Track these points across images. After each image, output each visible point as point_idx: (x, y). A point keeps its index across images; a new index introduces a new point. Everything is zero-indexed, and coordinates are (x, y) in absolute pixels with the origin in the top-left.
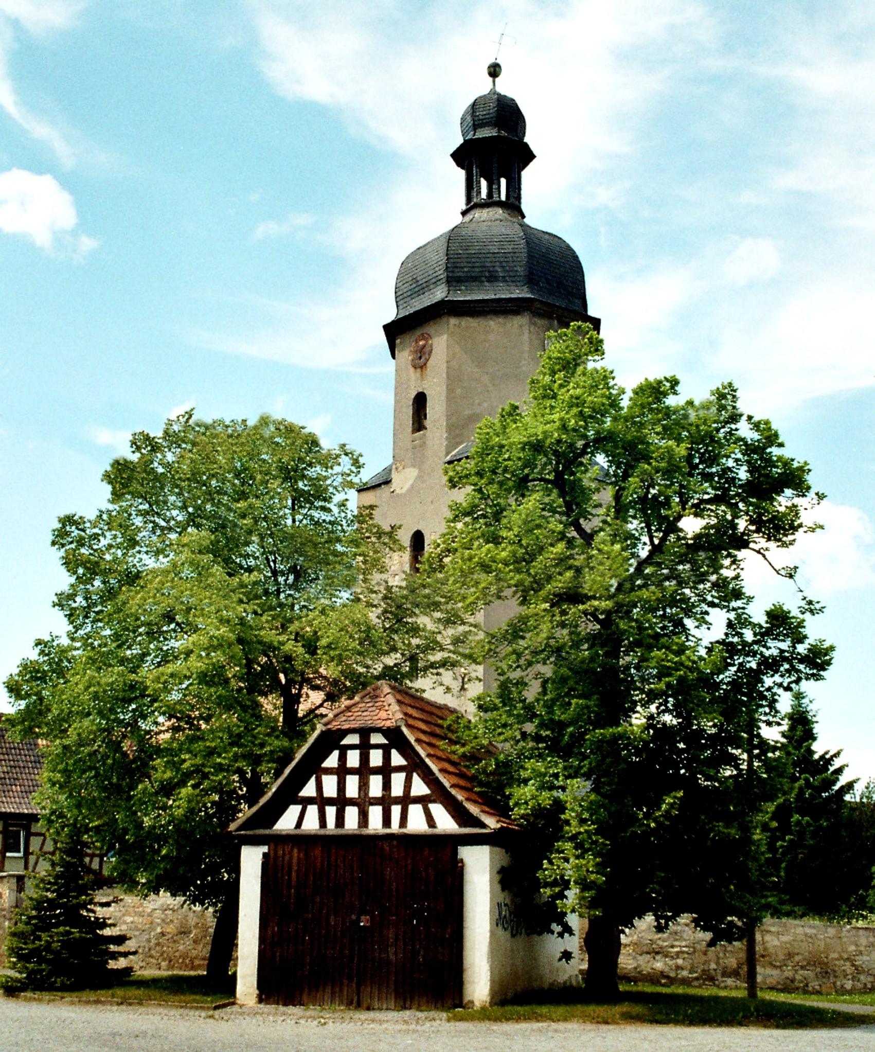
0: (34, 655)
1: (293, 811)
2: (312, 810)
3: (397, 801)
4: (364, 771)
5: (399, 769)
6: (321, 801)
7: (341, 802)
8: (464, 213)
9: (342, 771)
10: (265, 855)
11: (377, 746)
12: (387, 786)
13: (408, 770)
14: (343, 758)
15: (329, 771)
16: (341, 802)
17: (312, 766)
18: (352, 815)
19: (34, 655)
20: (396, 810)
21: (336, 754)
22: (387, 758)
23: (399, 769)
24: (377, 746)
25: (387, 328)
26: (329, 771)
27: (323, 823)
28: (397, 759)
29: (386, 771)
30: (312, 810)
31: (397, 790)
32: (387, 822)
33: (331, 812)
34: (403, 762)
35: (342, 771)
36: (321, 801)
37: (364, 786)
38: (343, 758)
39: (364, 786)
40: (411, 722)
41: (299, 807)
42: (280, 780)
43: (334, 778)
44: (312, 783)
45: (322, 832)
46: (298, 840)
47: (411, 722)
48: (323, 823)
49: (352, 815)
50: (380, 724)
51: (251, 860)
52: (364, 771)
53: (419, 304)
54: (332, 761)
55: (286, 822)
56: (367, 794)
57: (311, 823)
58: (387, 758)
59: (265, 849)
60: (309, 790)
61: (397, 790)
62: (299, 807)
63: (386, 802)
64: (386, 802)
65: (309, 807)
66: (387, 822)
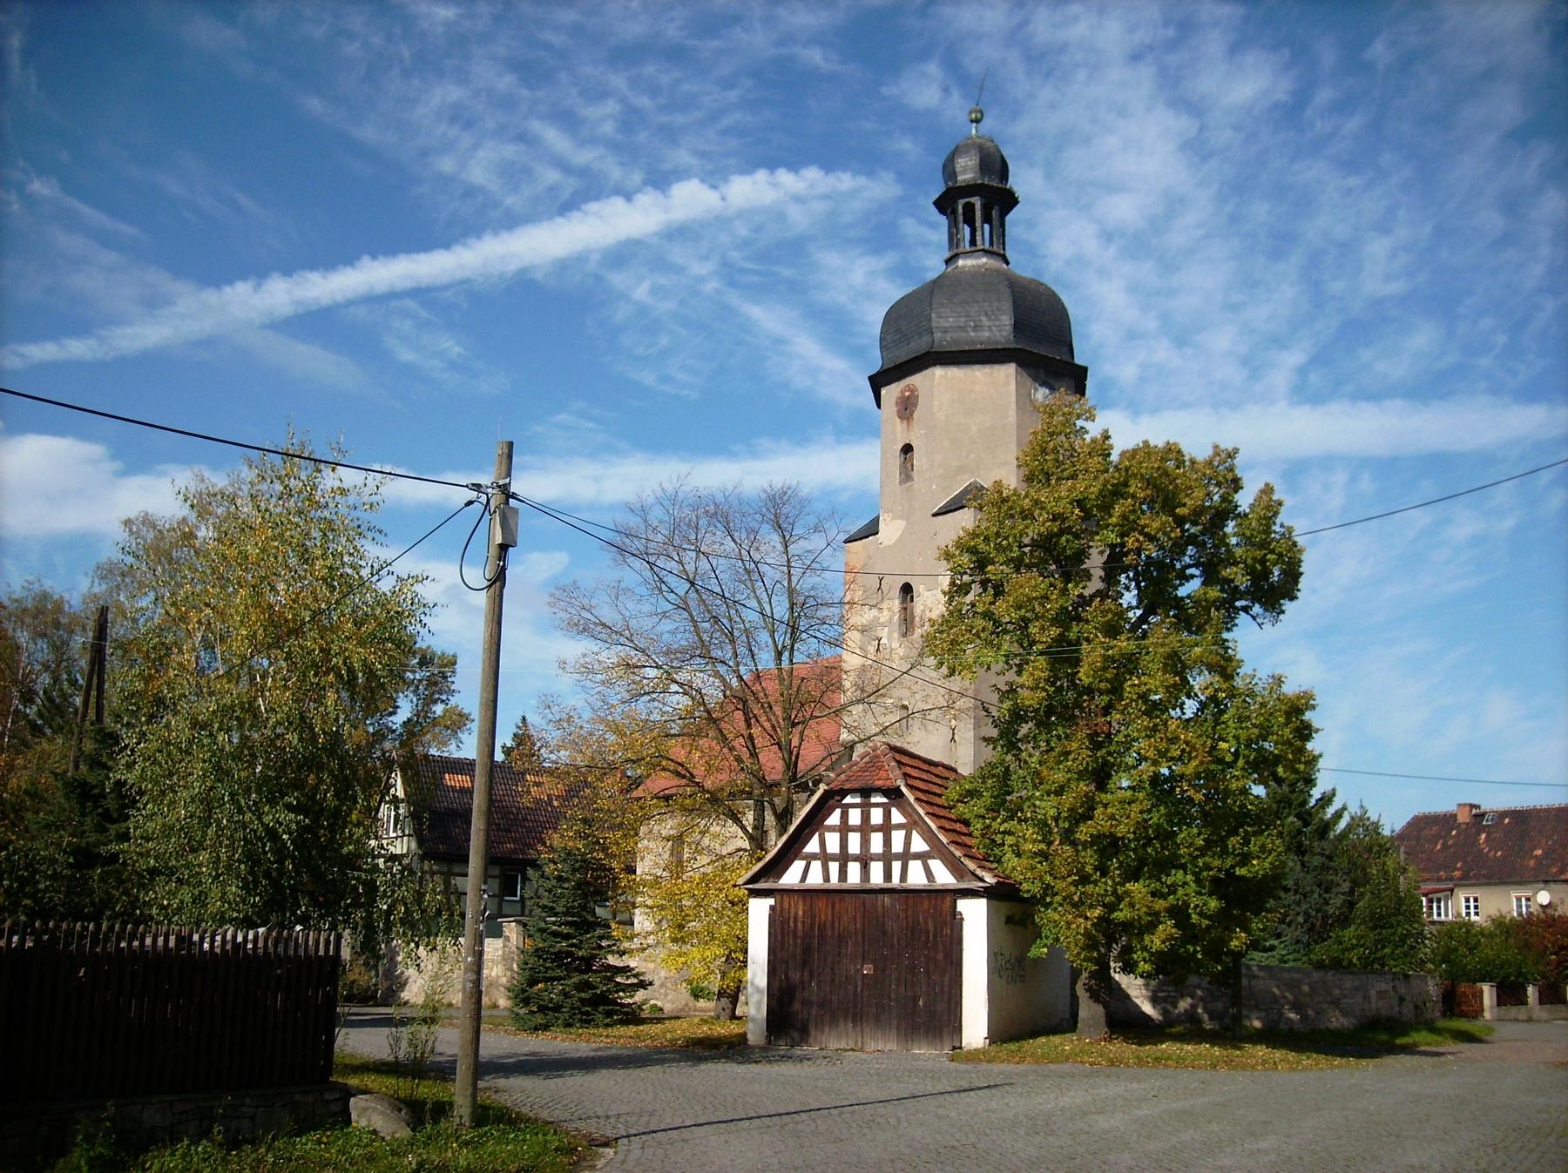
0: (962, 534)
1: (798, 866)
2: (816, 866)
3: (897, 857)
4: (865, 829)
5: (899, 827)
6: (825, 858)
7: (844, 858)
8: (948, 262)
9: (844, 829)
10: (772, 908)
11: (877, 805)
12: (887, 842)
13: (908, 828)
14: (844, 816)
15: (832, 829)
16: (844, 858)
17: (814, 822)
18: (854, 870)
19: (962, 534)
20: (896, 866)
21: (838, 812)
22: (887, 816)
23: (899, 827)
24: (877, 805)
25: (871, 378)
26: (832, 829)
27: (827, 878)
28: (897, 817)
29: (886, 828)
30: (816, 866)
31: (897, 846)
32: (888, 876)
33: (834, 867)
34: (904, 821)
35: (844, 829)
36: (825, 858)
37: (865, 842)
38: (844, 816)
39: (865, 842)
40: (911, 782)
41: (804, 863)
42: (785, 838)
43: (880, 835)
44: (815, 841)
45: (826, 886)
46: (807, 894)
47: (911, 782)
48: (827, 878)
49: (854, 870)
50: (879, 783)
51: (759, 911)
52: (865, 829)
53: (902, 355)
54: (834, 819)
55: (791, 877)
56: (868, 849)
57: (815, 878)
58: (887, 816)
59: (771, 901)
60: (813, 846)
61: (897, 846)
62: (804, 863)
63: (887, 858)
64: (887, 858)
65: (911, 863)
66: (888, 876)
